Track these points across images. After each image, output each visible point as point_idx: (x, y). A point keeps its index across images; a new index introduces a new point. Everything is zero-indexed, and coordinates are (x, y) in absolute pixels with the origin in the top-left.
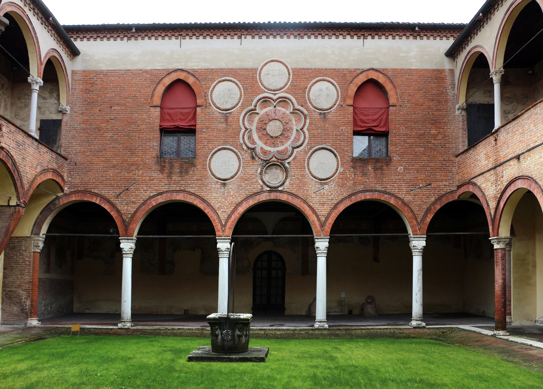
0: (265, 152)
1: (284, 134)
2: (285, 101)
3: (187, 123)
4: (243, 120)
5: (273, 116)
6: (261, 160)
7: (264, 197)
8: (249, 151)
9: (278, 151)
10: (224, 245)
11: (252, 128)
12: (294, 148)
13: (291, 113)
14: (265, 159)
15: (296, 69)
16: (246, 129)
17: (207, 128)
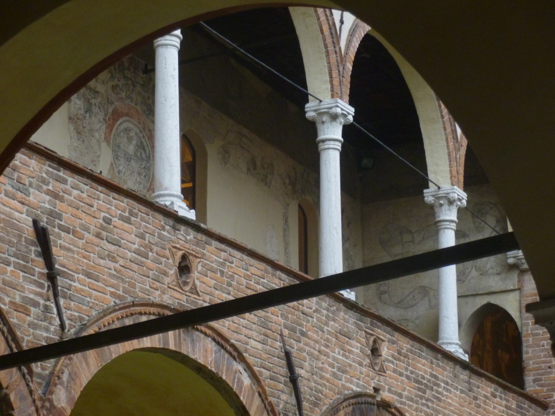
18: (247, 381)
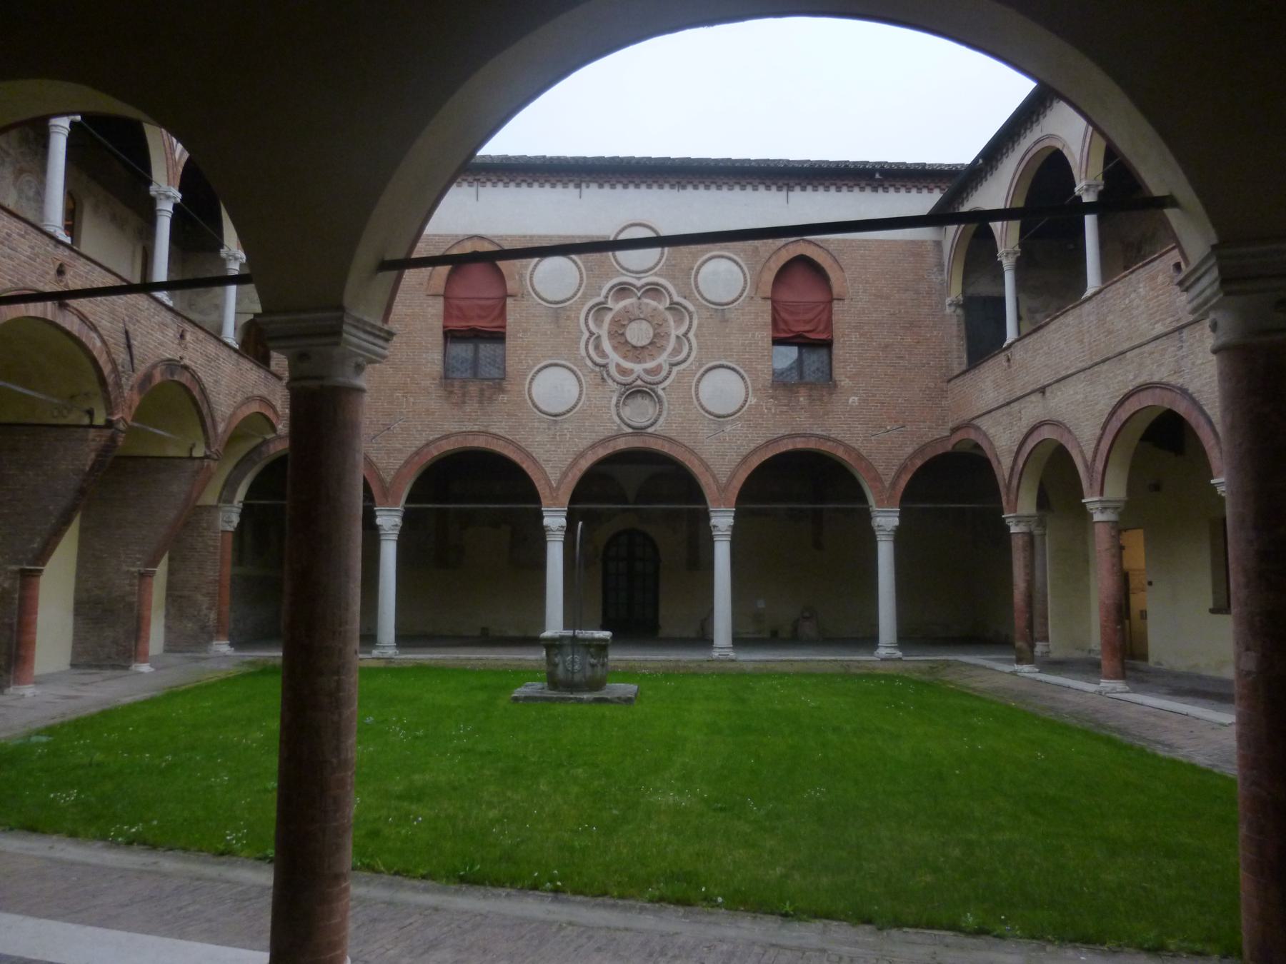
0: (623, 372)
1: (655, 345)
3: (493, 320)
4: (586, 319)
5: (637, 312)
7: (621, 444)
8: (597, 369)
9: (647, 372)
10: (554, 521)
13: (668, 309)
16: (592, 334)
17: (525, 331)
18: (98, 343)
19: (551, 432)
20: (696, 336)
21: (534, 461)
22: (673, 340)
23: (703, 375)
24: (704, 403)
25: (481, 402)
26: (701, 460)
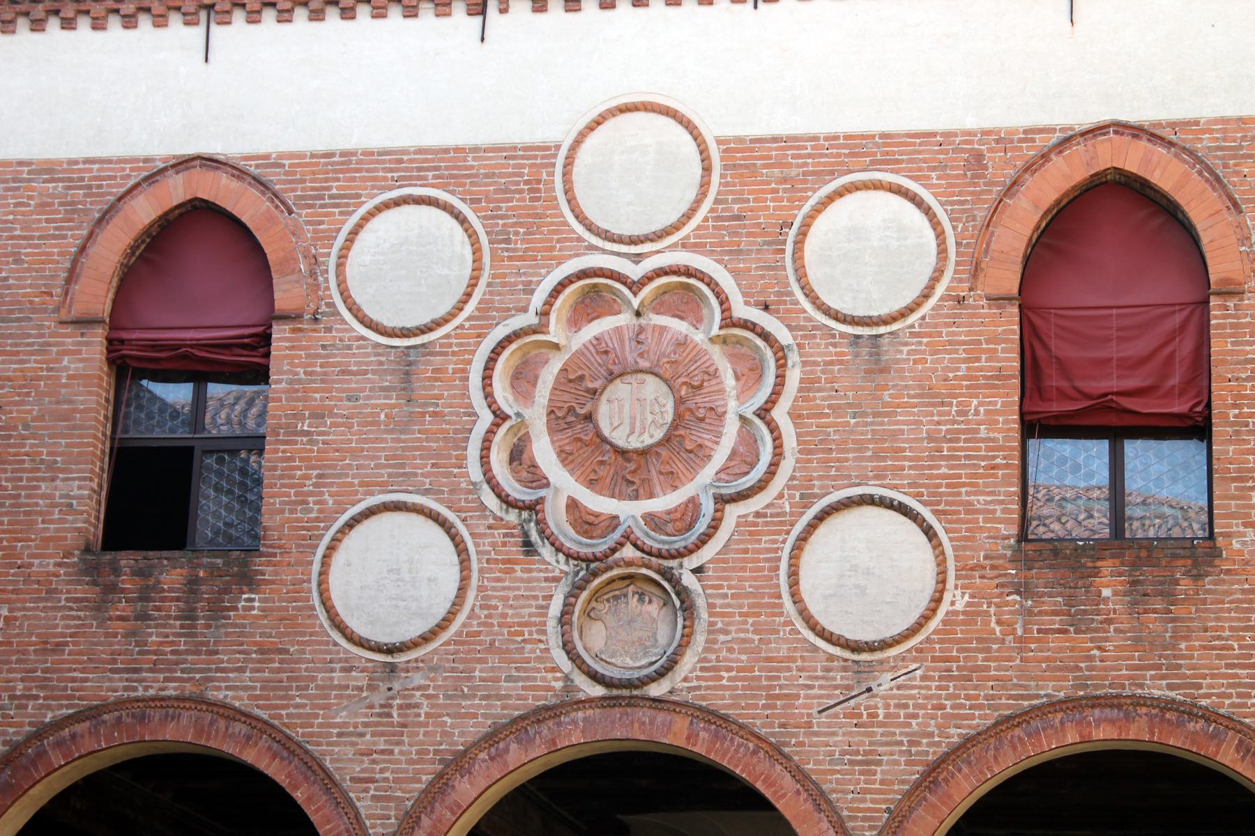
2: (688, 287)
4: (487, 378)
5: (630, 357)
6: (568, 556)
8: (512, 517)
11: (527, 413)
12: (723, 501)
14: (584, 551)
15: (739, 140)
16: (500, 417)
17: (318, 416)
19: (378, 698)
20: (795, 415)
21: (329, 783)
22: (731, 428)
23: (812, 527)
24: (815, 609)
25: (189, 616)
26: (800, 775)
